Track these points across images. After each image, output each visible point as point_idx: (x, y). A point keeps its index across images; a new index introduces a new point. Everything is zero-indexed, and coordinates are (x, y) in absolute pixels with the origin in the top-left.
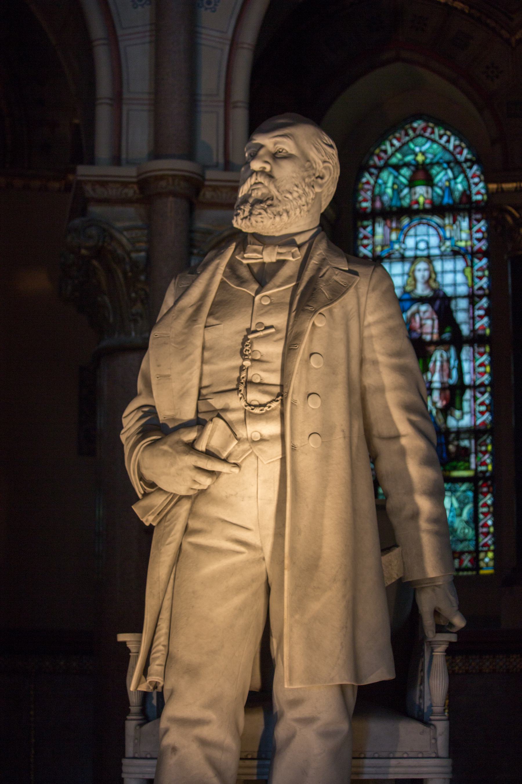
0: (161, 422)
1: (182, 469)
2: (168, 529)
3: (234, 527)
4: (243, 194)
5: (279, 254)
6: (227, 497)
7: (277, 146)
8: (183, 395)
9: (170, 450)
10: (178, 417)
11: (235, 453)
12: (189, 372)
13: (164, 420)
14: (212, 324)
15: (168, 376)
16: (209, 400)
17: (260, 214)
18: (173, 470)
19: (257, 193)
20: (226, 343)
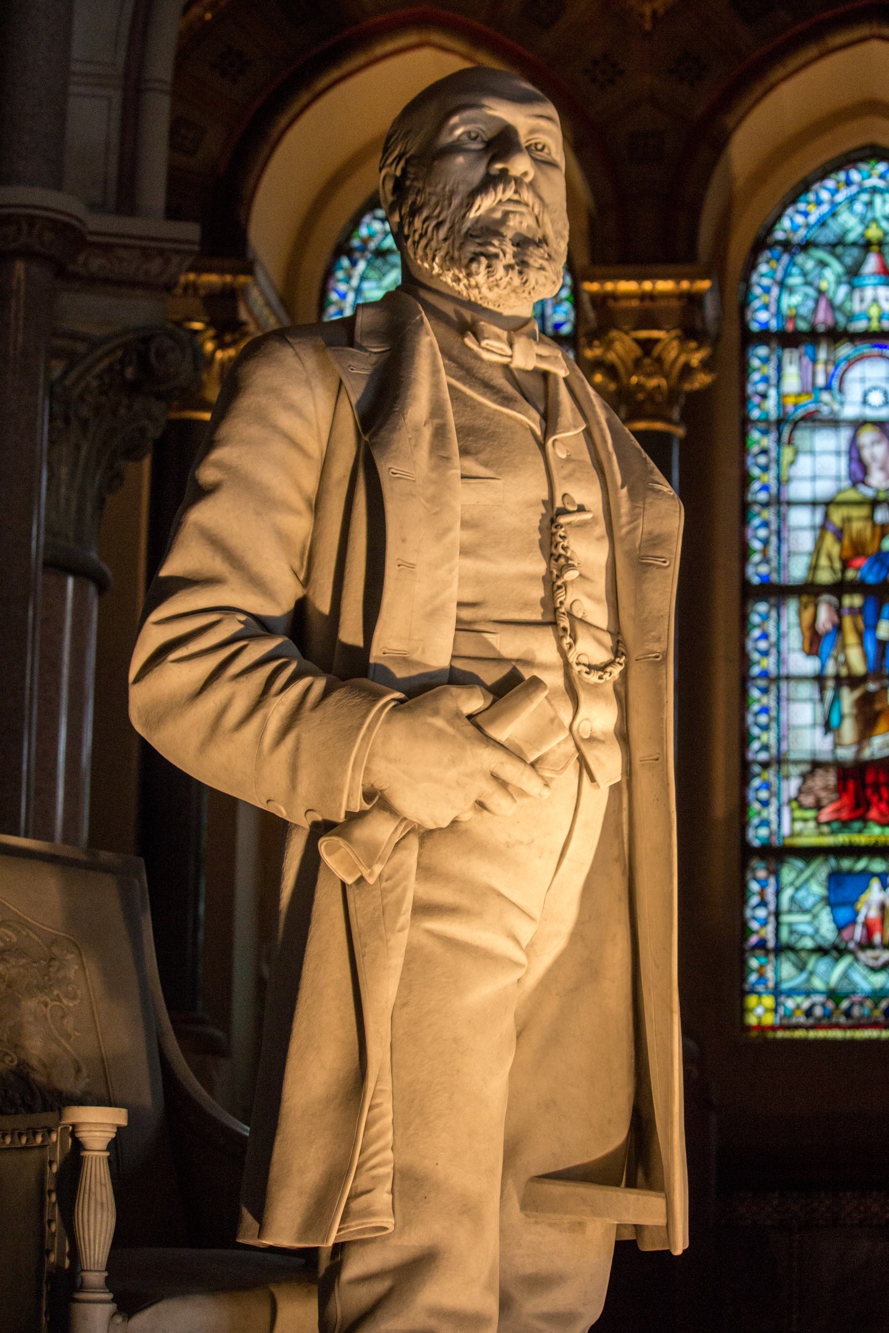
0: (372, 661)
1: (471, 775)
2: (391, 897)
3: (516, 909)
4: (478, 214)
5: (540, 357)
6: (508, 845)
7: (536, 136)
8: (433, 614)
9: (450, 730)
10: (416, 657)
11: (552, 758)
12: (447, 566)
13: (380, 658)
14: (474, 474)
15: (412, 566)
16: (486, 635)
17: (542, 268)
18: (452, 774)
19: (521, 223)
20: (511, 521)
